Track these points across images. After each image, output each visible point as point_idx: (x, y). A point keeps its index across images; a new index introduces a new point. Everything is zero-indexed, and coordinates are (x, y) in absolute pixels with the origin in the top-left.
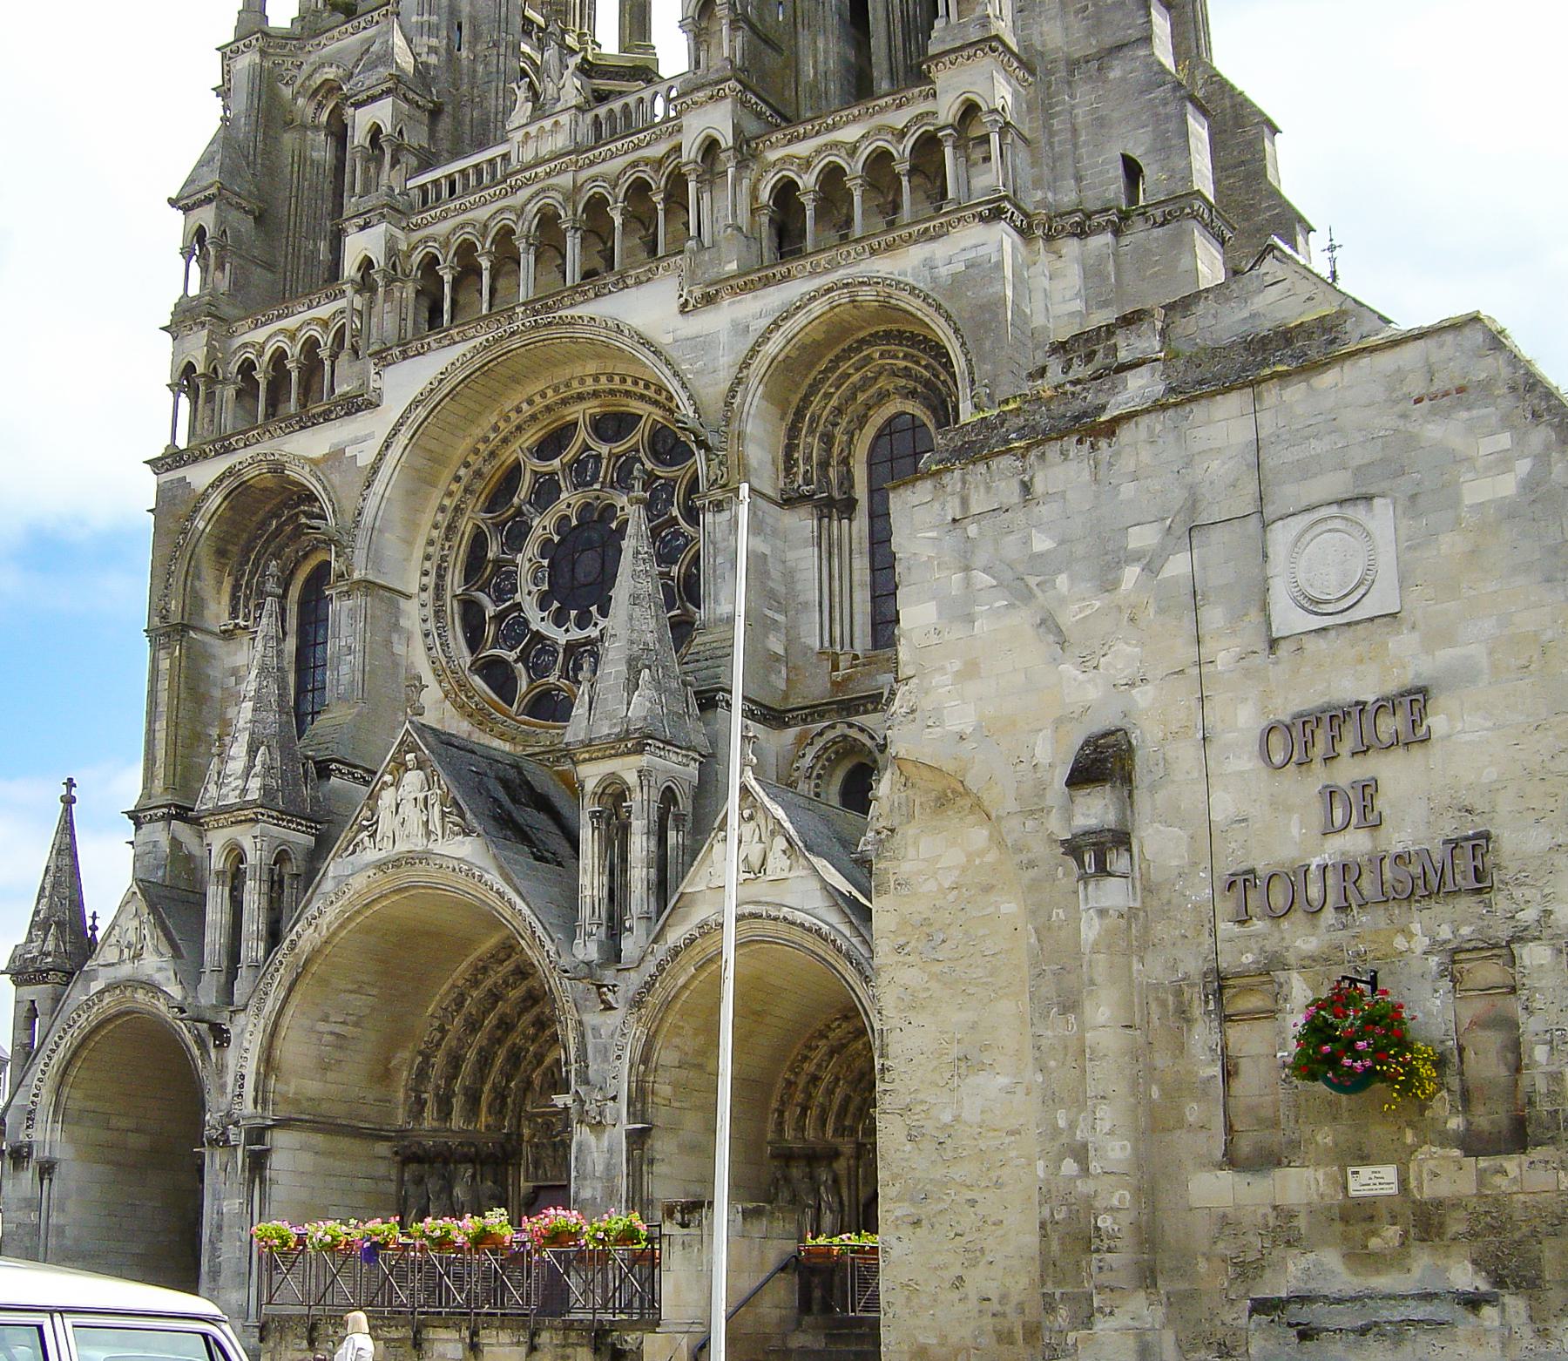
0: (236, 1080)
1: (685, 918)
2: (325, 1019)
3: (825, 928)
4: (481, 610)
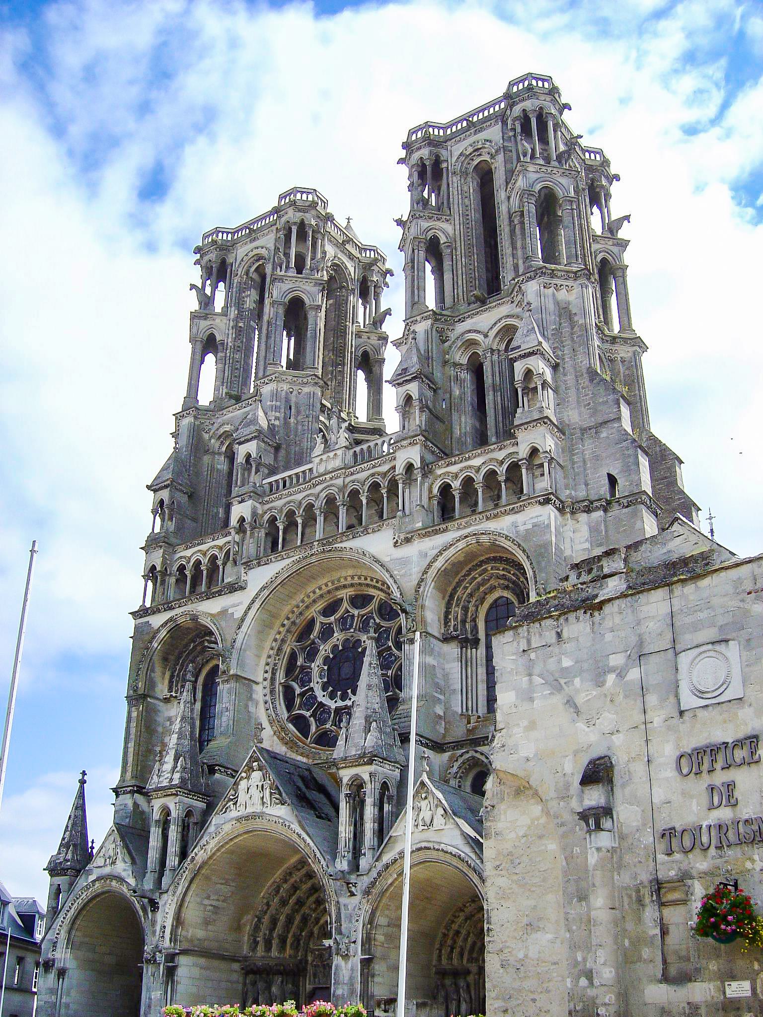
0: (161, 929)
1: (392, 848)
2: (208, 898)
3: (463, 855)
4: (293, 690)
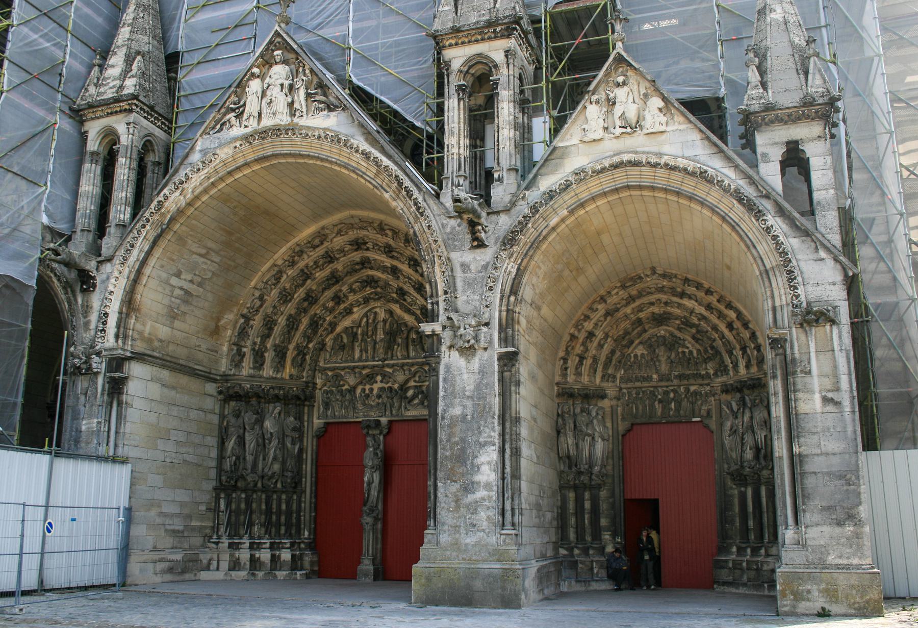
0: (100, 317)
2: (178, 275)
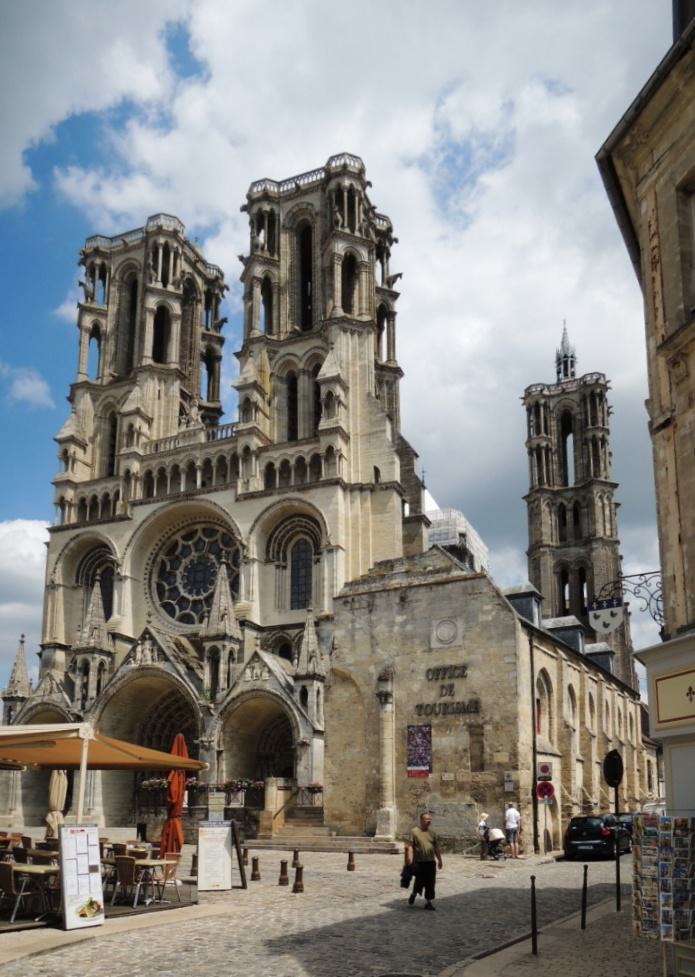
4: (164, 587)
